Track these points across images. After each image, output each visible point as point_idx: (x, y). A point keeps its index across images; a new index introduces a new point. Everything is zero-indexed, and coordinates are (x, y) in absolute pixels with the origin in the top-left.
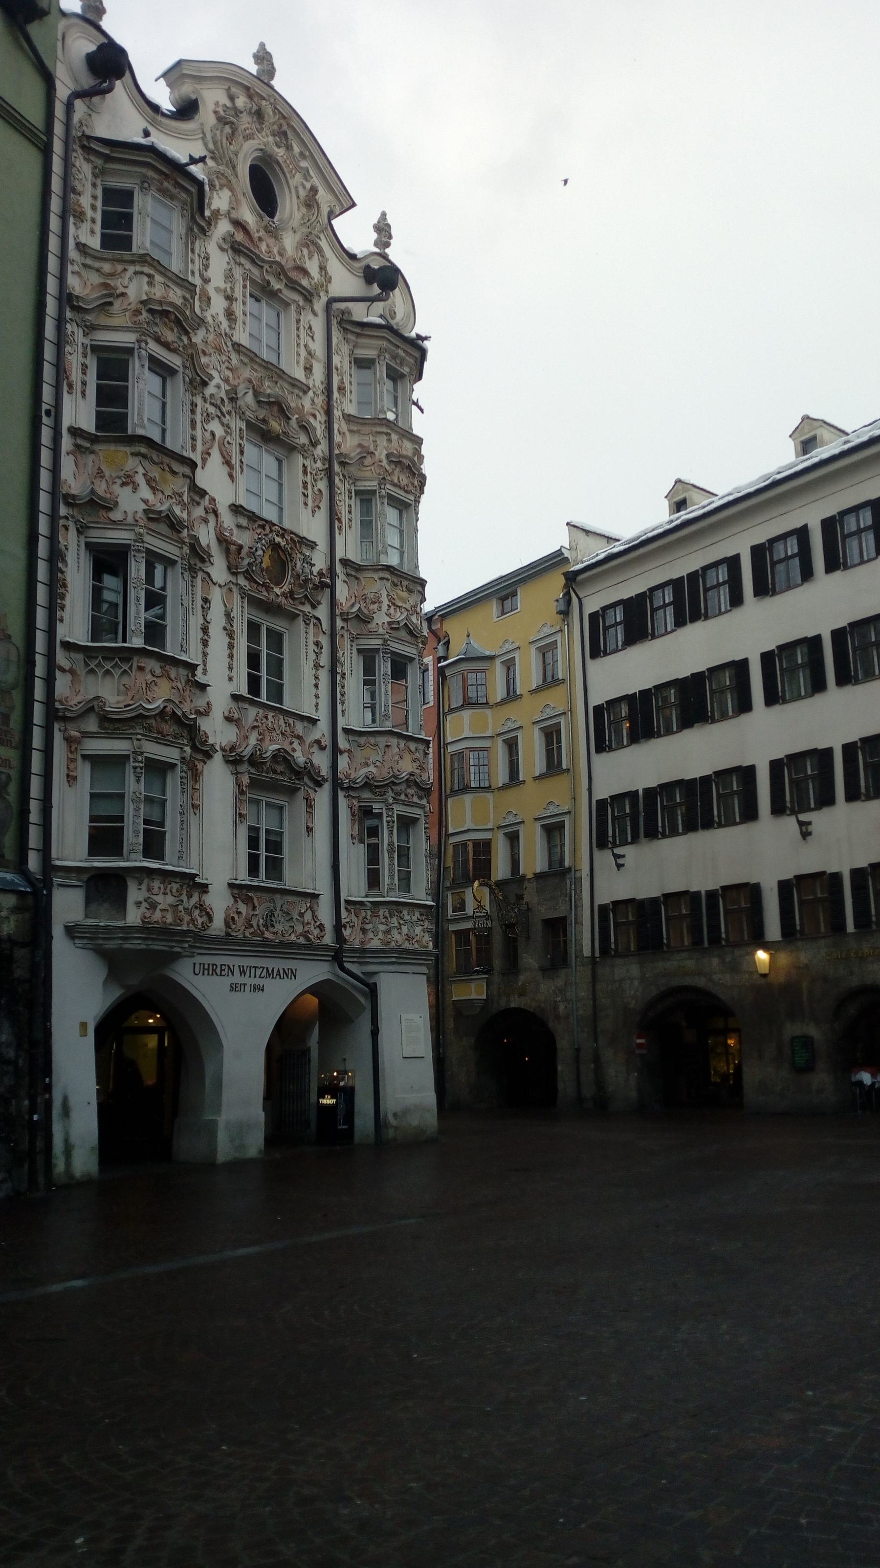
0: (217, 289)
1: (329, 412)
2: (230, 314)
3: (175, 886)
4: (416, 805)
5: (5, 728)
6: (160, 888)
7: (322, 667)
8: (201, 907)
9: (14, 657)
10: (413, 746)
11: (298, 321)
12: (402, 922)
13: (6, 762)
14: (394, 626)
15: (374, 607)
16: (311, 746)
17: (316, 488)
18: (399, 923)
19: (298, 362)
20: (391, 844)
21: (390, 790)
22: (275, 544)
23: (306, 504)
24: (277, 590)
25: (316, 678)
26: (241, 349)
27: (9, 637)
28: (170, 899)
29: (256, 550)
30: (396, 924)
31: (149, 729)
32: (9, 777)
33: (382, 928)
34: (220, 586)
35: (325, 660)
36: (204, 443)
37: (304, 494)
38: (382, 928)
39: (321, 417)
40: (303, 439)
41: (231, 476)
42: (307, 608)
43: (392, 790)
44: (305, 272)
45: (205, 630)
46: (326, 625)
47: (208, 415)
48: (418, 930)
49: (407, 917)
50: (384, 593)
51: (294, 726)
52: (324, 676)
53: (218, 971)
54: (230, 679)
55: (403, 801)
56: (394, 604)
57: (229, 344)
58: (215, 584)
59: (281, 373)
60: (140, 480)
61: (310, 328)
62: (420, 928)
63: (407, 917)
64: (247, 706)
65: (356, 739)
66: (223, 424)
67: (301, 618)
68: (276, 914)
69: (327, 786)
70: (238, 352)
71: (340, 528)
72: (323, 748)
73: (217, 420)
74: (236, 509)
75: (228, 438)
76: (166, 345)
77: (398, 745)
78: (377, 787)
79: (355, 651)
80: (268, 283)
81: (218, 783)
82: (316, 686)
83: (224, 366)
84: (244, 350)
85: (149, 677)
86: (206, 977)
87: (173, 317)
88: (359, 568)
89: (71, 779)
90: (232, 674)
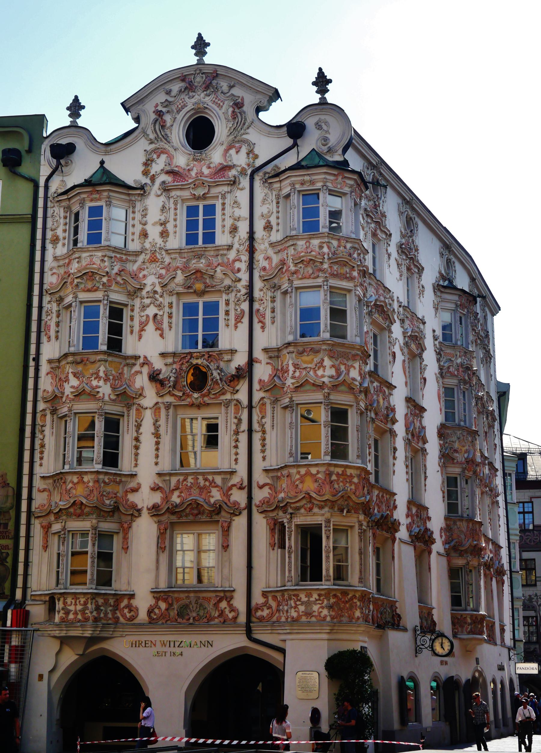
0: (154, 224)
1: (252, 250)
2: (164, 234)
3: (82, 600)
4: (314, 514)
5: (6, 530)
6: (72, 602)
7: (243, 432)
8: (129, 607)
9: (11, 493)
10: (314, 471)
11: (223, 204)
12: (298, 603)
13: (6, 547)
14: (296, 385)
15: (286, 375)
16: (230, 488)
17: (239, 310)
18: (296, 604)
19: (223, 232)
20: (290, 547)
21: (289, 508)
22: (195, 365)
23: (227, 326)
24: (196, 395)
25: (237, 441)
26: (170, 252)
27: (8, 484)
28: (79, 607)
29: (170, 378)
30: (293, 605)
31: (69, 515)
32: (8, 554)
33: (286, 608)
34: (150, 408)
35: (244, 426)
36: (141, 323)
37: (225, 319)
38: (286, 608)
39: (245, 258)
40: (227, 282)
41: (162, 335)
42: (228, 396)
43: (291, 507)
44: (230, 167)
45: (137, 439)
46: (245, 402)
47: (144, 307)
48: (316, 608)
49: (304, 599)
50: (290, 362)
51: (213, 480)
52: (243, 438)
53: (143, 644)
54: (156, 464)
55: (302, 514)
56: (298, 368)
57: (164, 253)
58: (147, 408)
59: (204, 249)
60: (71, 376)
61: (235, 202)
62: (319, 606)
63: (304, 599)
64: (167, 478)
65: (275, 474)
66: (156, 306)
67: (223, 404)
68: (191, 606)
69: (245, 513)
70: (169, 254)
71: (263, 328)
72: (241, 488)
73: (152, 305)
74: (163, 355)
75: (161, 313)
76: (89, 291)
77: (299, 473)
78: (282, 507)
79: (278, 409)
80: (194, 195)
81: (145, 530)
82: (236, 447)
83: (158, 269)
84: (172, 251)
85: (71, 485)
86: (137, 648)
87: (90, 274)
88: (279, 350)
89: (45, 547)
90: (158, 461)
